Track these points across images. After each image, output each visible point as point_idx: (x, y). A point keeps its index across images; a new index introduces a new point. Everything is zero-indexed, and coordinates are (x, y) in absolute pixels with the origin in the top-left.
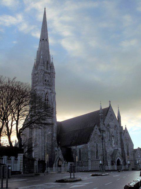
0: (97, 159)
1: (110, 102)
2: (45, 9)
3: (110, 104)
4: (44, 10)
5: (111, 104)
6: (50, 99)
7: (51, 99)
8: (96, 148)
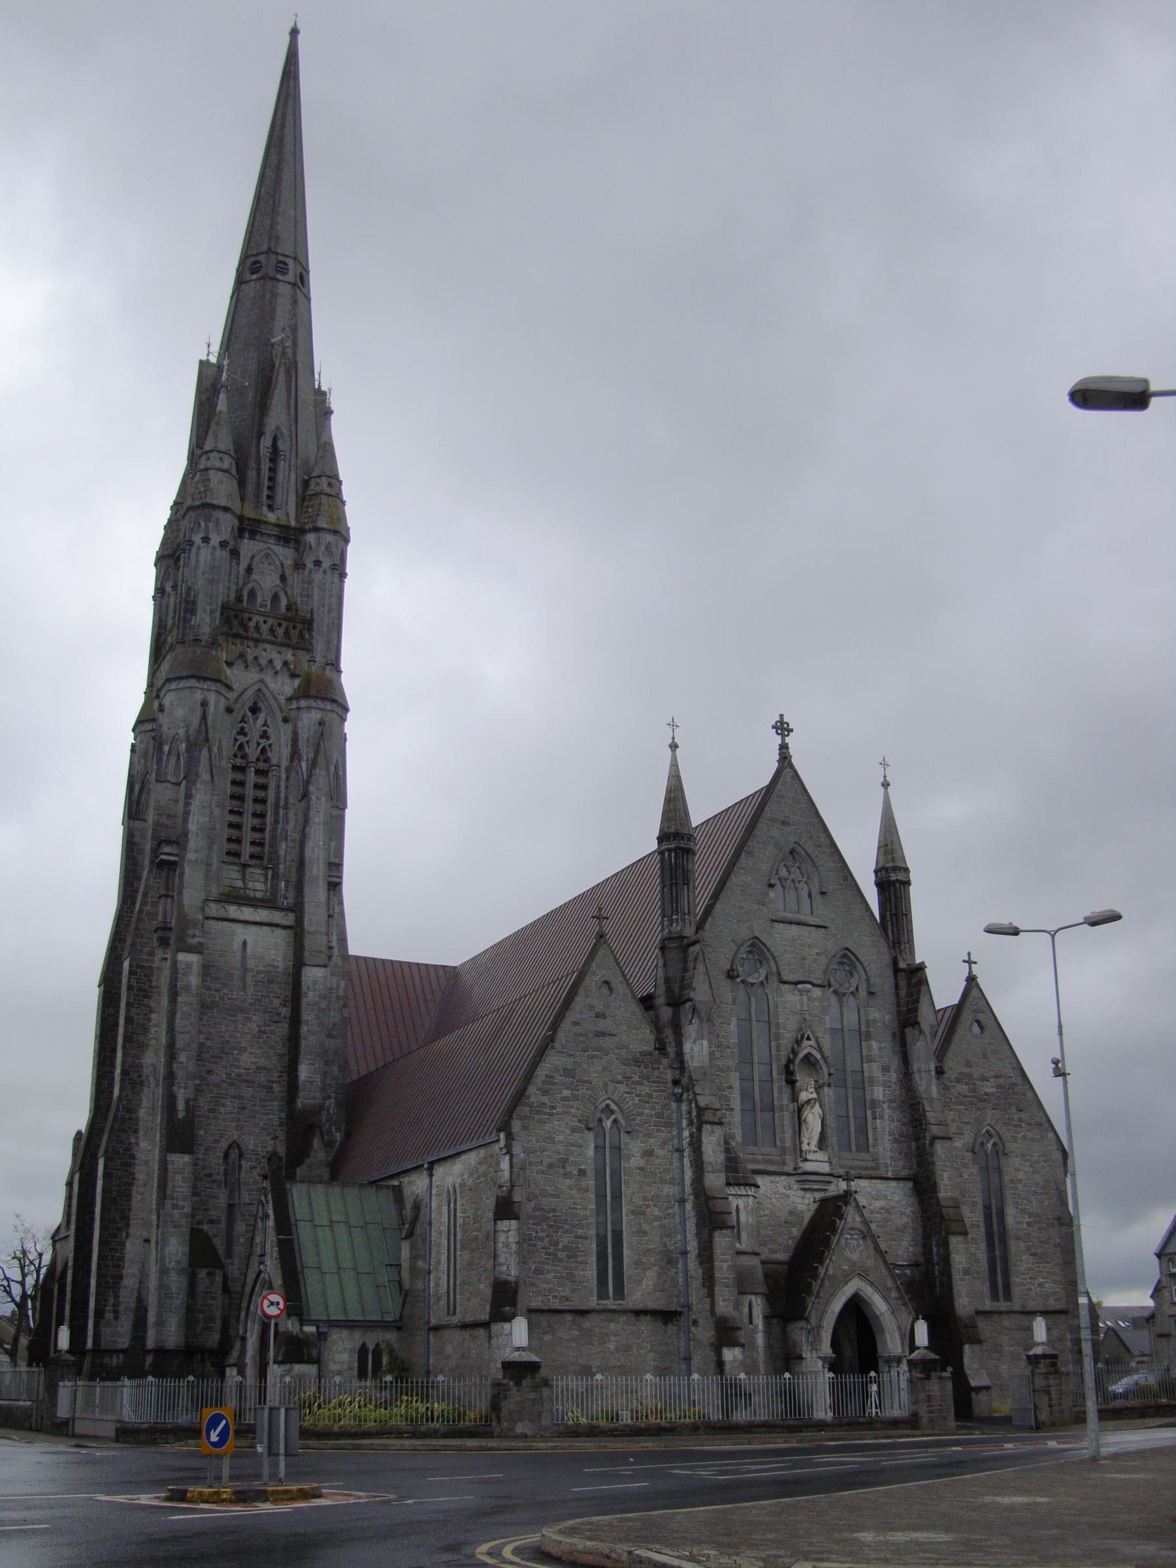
0: (602, 1295)
1: (782, 728)
2: (294, 33)
3: (784, 747)
4: (286, 39)
5: (792, 751)
6: (286, 752)
7: (295, 754)
8: (590, 1182)
